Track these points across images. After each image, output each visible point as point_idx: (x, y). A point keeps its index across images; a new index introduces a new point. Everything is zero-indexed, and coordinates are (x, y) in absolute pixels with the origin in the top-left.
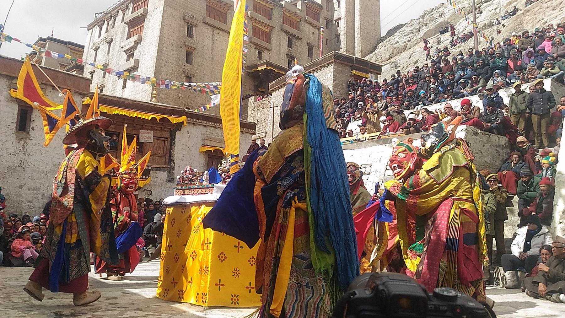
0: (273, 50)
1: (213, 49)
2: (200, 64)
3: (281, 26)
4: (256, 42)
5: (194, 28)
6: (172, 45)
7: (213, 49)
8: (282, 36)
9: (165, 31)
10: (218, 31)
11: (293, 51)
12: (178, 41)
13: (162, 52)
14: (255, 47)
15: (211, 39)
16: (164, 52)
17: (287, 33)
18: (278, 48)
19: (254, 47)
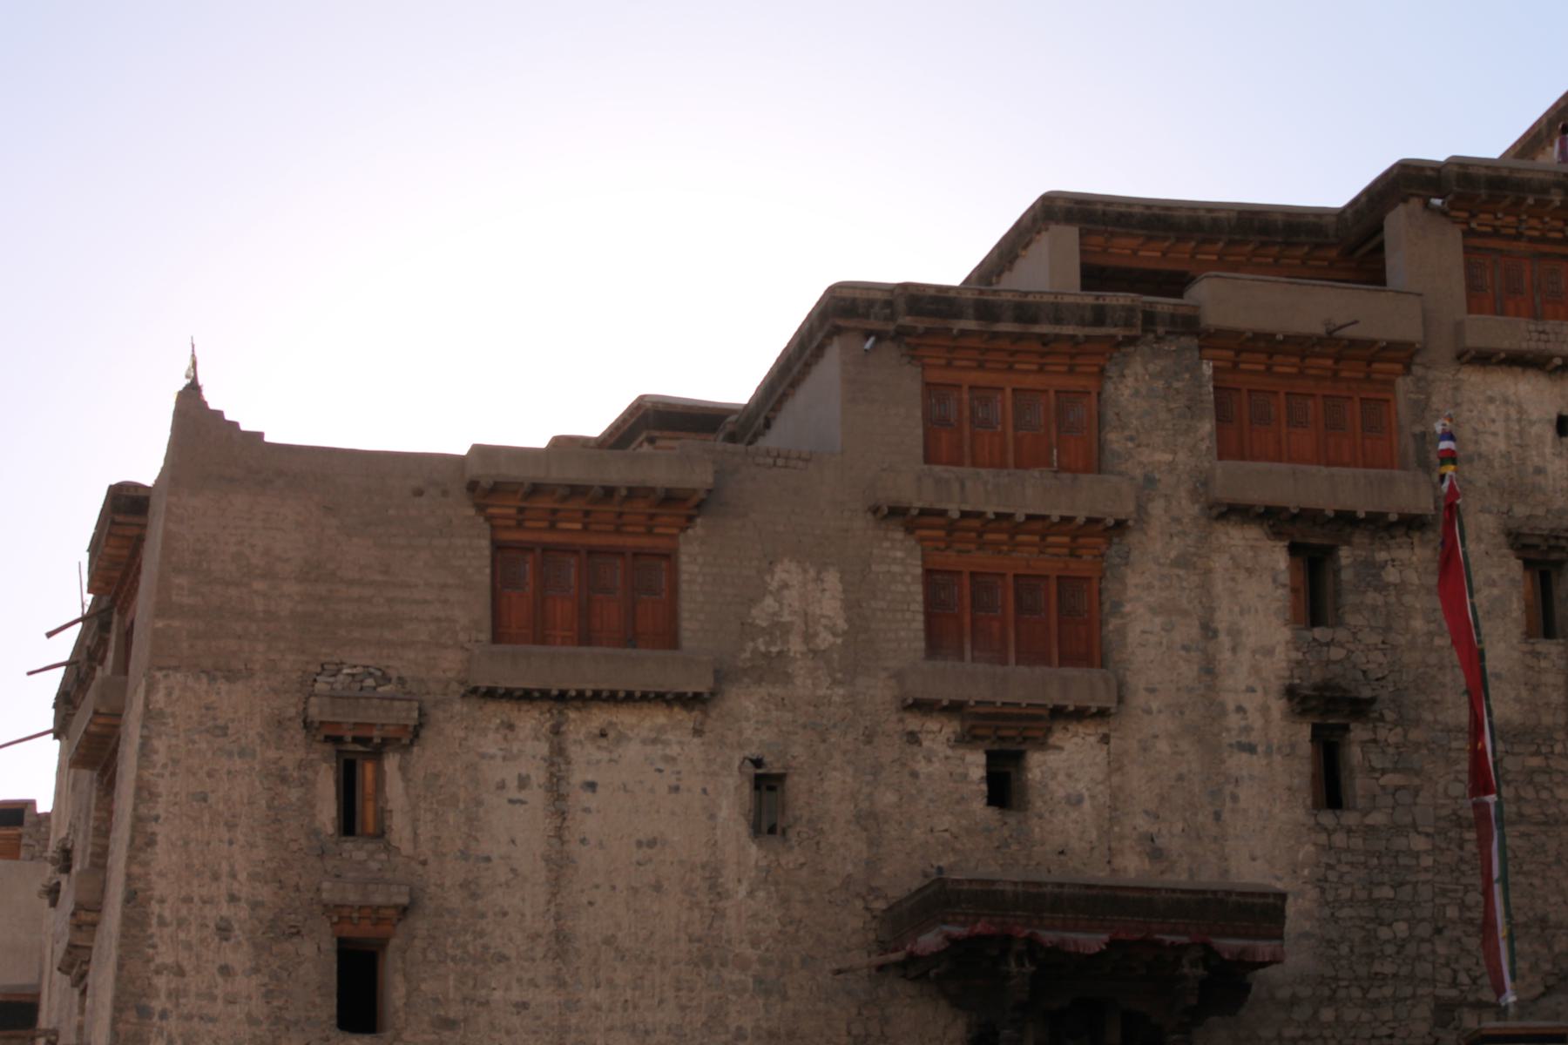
0: (1139, 699)
1: (559, 866)
2: (454, 1011)
3: (1202, 483)
4: (947, 694)
5: (391, 763)
6: (224, 930)
7: (559, 866)
8: (1220, 563)
9: (163, 857)
10: (599, 717)
11: (1355, 646)
12: (265, 892)
13: (144, 1013)
14: (951, 727)
15: (536, 797)
16: (157, 1005)
17: (1273, 519)
18: (1189, 671)
19: (938, 733)
